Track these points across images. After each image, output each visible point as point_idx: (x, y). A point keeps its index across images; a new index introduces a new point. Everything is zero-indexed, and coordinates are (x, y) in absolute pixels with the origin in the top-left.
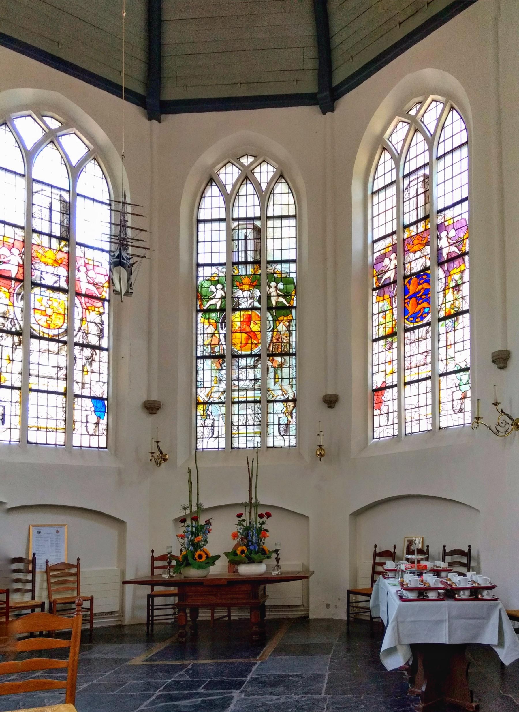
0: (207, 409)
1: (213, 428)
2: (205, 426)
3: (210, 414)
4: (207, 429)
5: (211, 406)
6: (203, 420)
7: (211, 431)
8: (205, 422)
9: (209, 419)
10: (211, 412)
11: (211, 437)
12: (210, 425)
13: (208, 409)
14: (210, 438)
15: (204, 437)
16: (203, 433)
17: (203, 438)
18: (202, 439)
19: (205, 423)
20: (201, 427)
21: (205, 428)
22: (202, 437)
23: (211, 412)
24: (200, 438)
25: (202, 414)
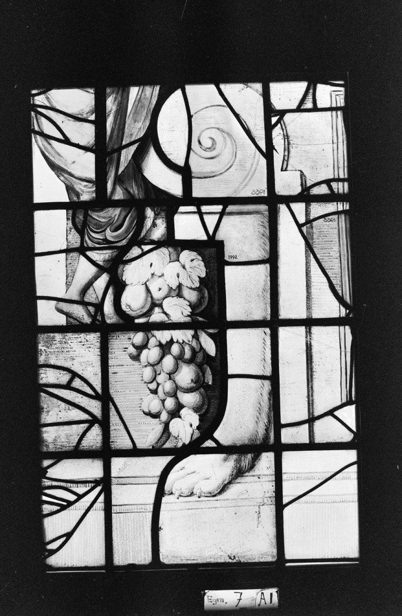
0: (136, 129)
1: (210, 346)
2: (127, 323)
3: (172, 184)
4: (151, 354)
5: (176, 98)
6: (99, 257)
7: (186, 375)
8: (133, 273)
9: (170, 242)
10: (185, 172)
11: (194, 448)
12: (178, 310)
13: (150, 139)
14: (180, 454)
15: (120, 440)
16: (105, 398)
17: (106, 453)
18: (92, 469)
19: (118, 286)
20: (74, 327)
21: (121, 345)
22: (94, 438)
23: (185, 172)
24: (77, 453)
25: (87, 194)
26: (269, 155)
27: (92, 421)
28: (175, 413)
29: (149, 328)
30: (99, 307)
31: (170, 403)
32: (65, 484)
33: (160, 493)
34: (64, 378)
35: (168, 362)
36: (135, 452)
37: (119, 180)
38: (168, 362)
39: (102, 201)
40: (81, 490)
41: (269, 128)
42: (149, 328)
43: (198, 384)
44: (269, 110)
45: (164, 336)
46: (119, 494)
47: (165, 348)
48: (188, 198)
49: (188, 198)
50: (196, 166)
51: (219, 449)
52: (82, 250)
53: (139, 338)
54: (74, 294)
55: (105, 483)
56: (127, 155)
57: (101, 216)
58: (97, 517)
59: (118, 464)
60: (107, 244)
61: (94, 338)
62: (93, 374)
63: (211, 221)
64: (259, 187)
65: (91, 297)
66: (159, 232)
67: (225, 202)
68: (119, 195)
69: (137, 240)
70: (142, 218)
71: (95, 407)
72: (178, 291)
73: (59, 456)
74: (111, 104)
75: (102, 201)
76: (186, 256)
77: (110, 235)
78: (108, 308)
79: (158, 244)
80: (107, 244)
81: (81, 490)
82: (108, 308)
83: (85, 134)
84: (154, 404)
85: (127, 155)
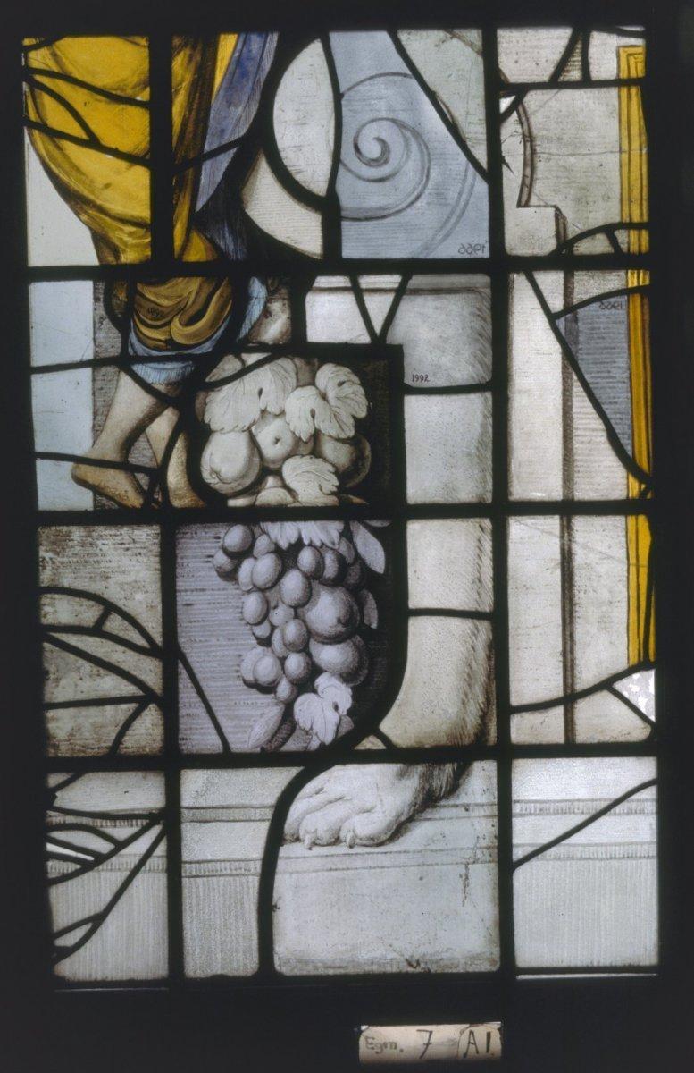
0: (232, 120)
1: (375, 555)
4: (261, 567)
6: (158, 375)
7: (327, 610)
10: (328, 208)
11: (343, 751)
14: (314, 762)
15: (200, 737)
16: (169, 652)
18: (145, 793)
19: (195, 433)
20: (109, 514)
22: (147, 731)
24: (115, 760)
25: (134, 248)
26: (493, 173)
27: (145, 698)
28: (305, 684)
29: (256, 517)
30: (158, 474)
31: (295, 663)
32: (93, 821)
33: (276, 838)
34: (89, 614)
35: (293, 584)
36: (228, 759)
37: (198, 222)
38: (293, 584)
39: (163, 264)
40: (122, 832)
41: (494, 121)
42: (256, 517)
43: (351, 628)
44: (495, 84)
45: (285, 533)
46: (198, 843)
47: (287, 557)
48: (332, 260)
49: (332, 260)
50: (352, 195)
51: (391, 753)
52: (124, 362)
53: (235, 536)
54: (108, 448)
55: (169, 820)
56: (212, 174)
57: (160, 295)
58: (151, 887)
59: (194, 784)
60: (173, 350)
61: (146, 535)
62: (144, 603)
63: (378, 306)
64: (471, 239)
65: (142, 455)
66: (275, 329)
67: (407, 267)
68: (198, 252)
69: (234, 339)
70: (240, 301)
71: (149, 669)
72: (312, 446)
73: (80, 766)
74: (181, 67)
75: (163, 264)
76: (328, 375)
77: (179, 331)
78: (175, 476)
79: (275, 352)
80: (173, 350)
81: (122, 832)
82: (175, 476)
83: (131, 128)
84: (264, 667)
85: (212, 174)
